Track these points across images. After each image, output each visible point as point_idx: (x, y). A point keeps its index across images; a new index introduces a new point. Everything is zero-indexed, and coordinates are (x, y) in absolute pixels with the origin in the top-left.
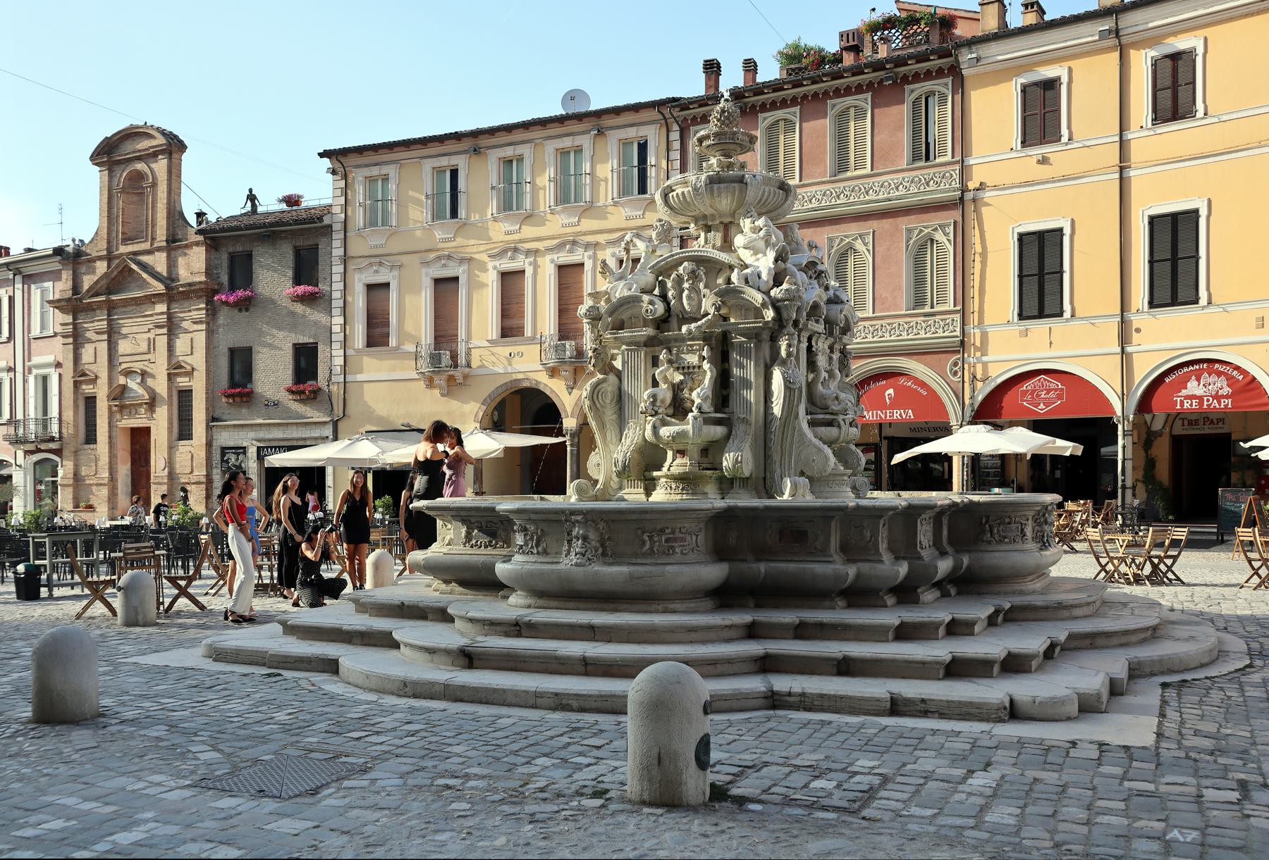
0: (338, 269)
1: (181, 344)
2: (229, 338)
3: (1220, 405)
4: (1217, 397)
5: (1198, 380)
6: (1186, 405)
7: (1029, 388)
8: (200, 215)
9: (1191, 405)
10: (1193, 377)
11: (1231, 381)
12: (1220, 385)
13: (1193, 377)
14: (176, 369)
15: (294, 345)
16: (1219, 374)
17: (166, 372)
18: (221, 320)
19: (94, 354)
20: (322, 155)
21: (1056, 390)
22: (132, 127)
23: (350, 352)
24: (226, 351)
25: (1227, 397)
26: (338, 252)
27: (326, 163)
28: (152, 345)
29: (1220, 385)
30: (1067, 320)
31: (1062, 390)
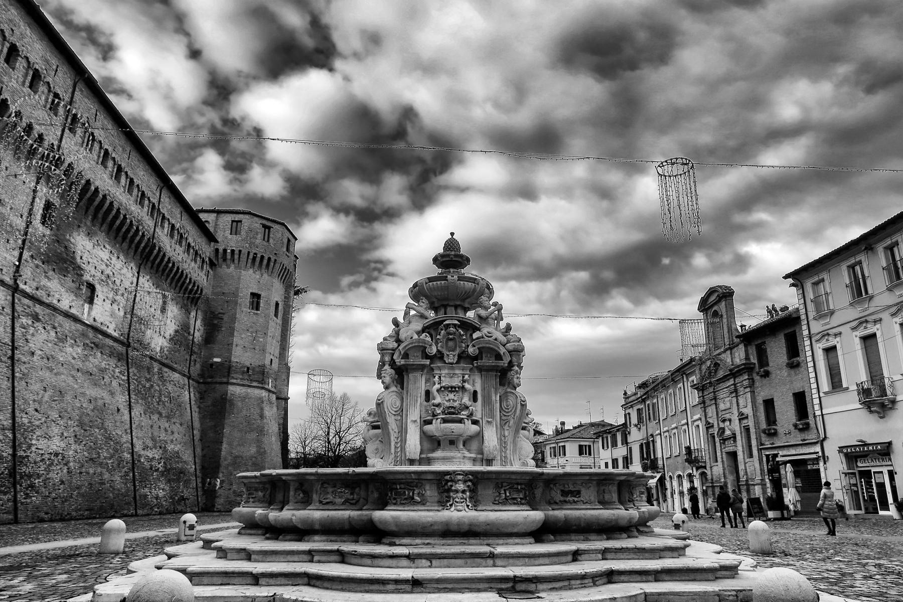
0: (807, 343)
1: (742, 401)
2: (763, 394)
8: (742, 326)
14: (742, 417)
15: (794, 394)
17: (737, 418)
18: (757, 384)
19: (711, 411)
20: (786, 277)
22: (710, 289)
23: (822, 395)
24: (762, 402)
26: (806, 333)
27: (791, 281)
28: (731, 403)
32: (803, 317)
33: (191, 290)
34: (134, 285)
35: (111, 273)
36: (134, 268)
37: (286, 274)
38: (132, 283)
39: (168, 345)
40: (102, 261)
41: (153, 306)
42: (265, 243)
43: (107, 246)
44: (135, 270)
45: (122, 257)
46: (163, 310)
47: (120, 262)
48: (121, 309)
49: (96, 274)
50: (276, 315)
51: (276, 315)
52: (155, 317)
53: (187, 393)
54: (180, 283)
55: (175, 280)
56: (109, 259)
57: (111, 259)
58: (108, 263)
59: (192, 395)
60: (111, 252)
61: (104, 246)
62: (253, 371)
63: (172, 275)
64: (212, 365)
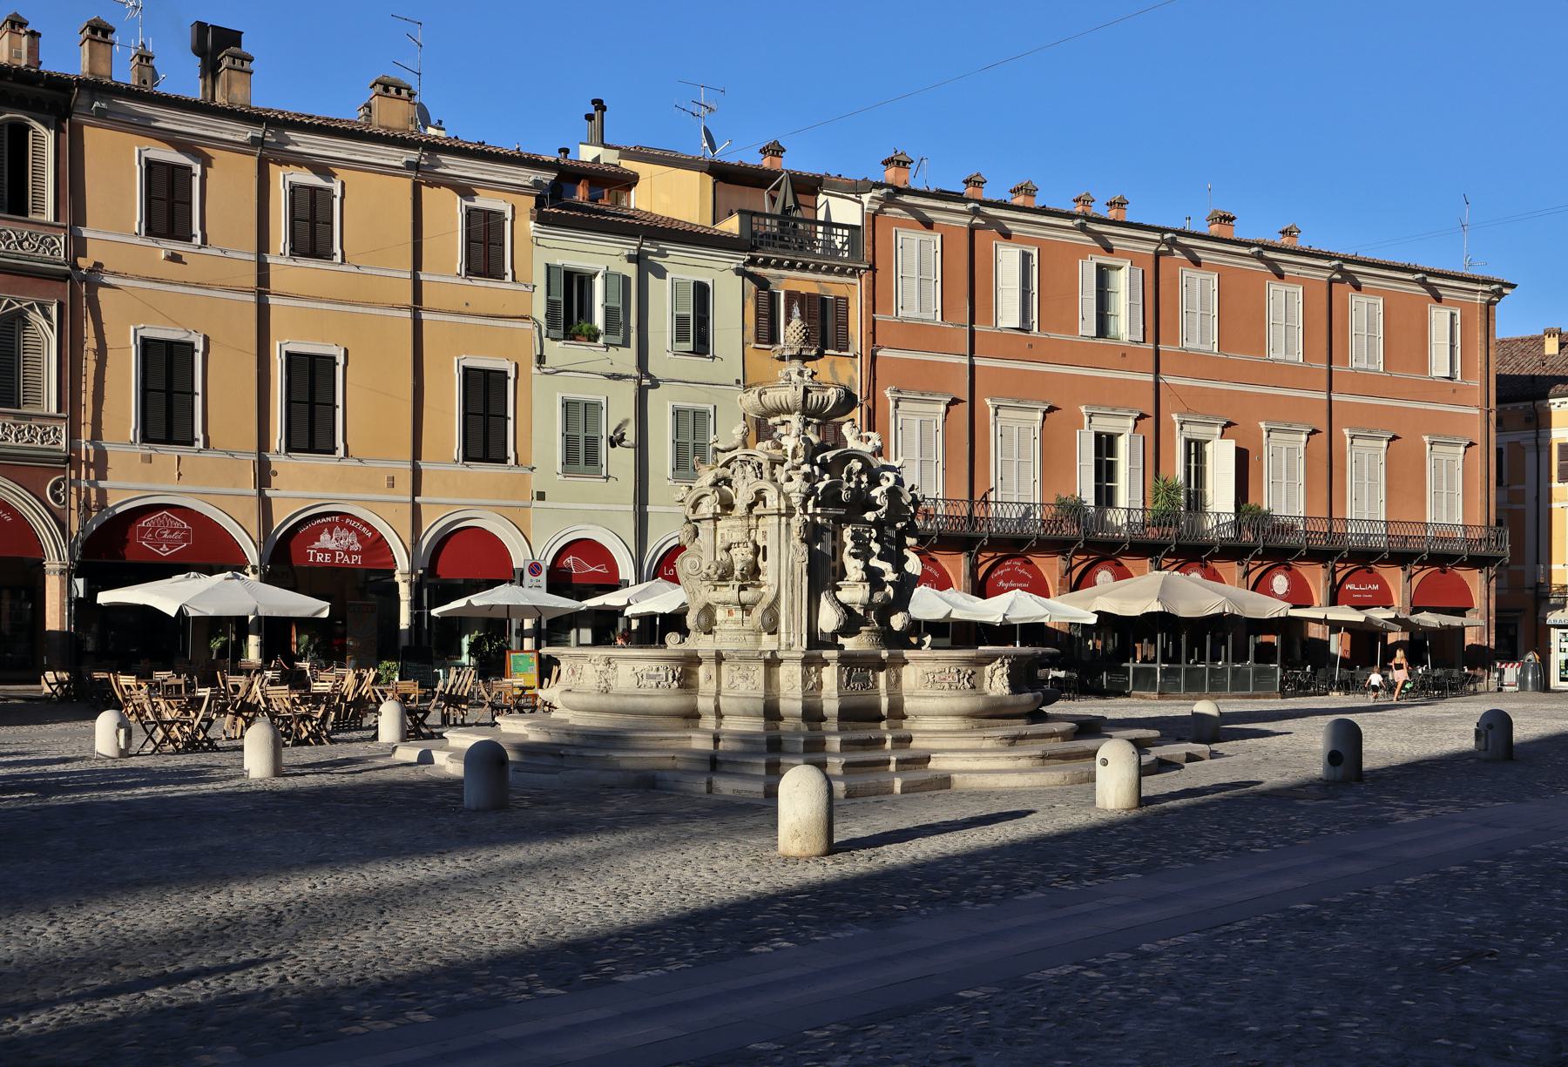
3: (351, 561)
4: (349, 553)
5: (331, 533)
6: (319, 559)
7: (149, 525)
9: (324, 559)
10: (326, 530)
11: (361, 538)
12: (350, 540)
13: (326, 530)
16: (350, 529)
21: (181, 530)
25: (357, 553)
29: (350, 540)
30: (199, 451)
31: (187, 530)
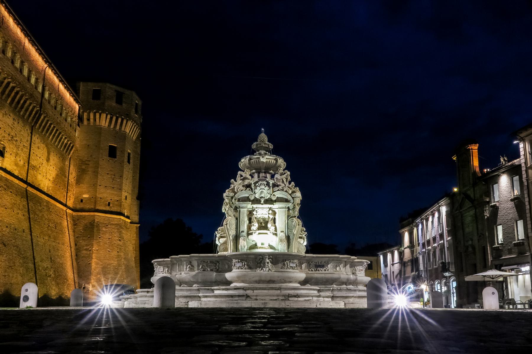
32: (523, 165)
33: (66, 144)
34: (29, 142)
35: (15, 134)
36: (28, 129)
37: (135, 129)
38: (27, 141)
39: (52, 185)
40: (9, 125)
41: (42, 157)
42: (118, 106)
43: (11, 115)
44: (29, 131)
45: (21, 122)
46: (48, 160)
47: (20, 126)
48: (21, 160)
49: (6, 136)
50: (129, 162)
51: (129, 162)
52: (43, 165)
53: (66, 221)
54: (59, 138)
55: (56, 137)
56: (13, 124)
57: (14, 124)
58: (12, 127)
59: (69, 222)
60: (14, 119)
61: (9, 115)
62: (113, 204)
63: (53, 133)
64: (82, 201)
